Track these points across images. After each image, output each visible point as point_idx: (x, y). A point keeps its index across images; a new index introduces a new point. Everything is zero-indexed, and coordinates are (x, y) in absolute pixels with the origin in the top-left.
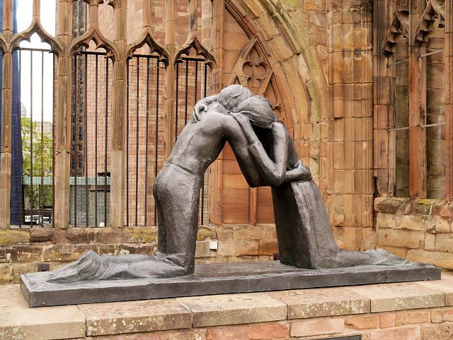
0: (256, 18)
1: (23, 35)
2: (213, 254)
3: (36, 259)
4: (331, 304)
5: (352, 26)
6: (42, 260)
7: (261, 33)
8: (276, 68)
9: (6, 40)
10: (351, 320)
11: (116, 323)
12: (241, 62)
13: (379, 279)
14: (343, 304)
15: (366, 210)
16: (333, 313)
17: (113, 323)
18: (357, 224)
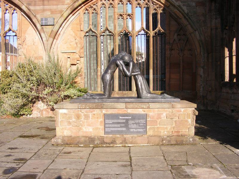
0: (180, 19)
5: (214, 20)
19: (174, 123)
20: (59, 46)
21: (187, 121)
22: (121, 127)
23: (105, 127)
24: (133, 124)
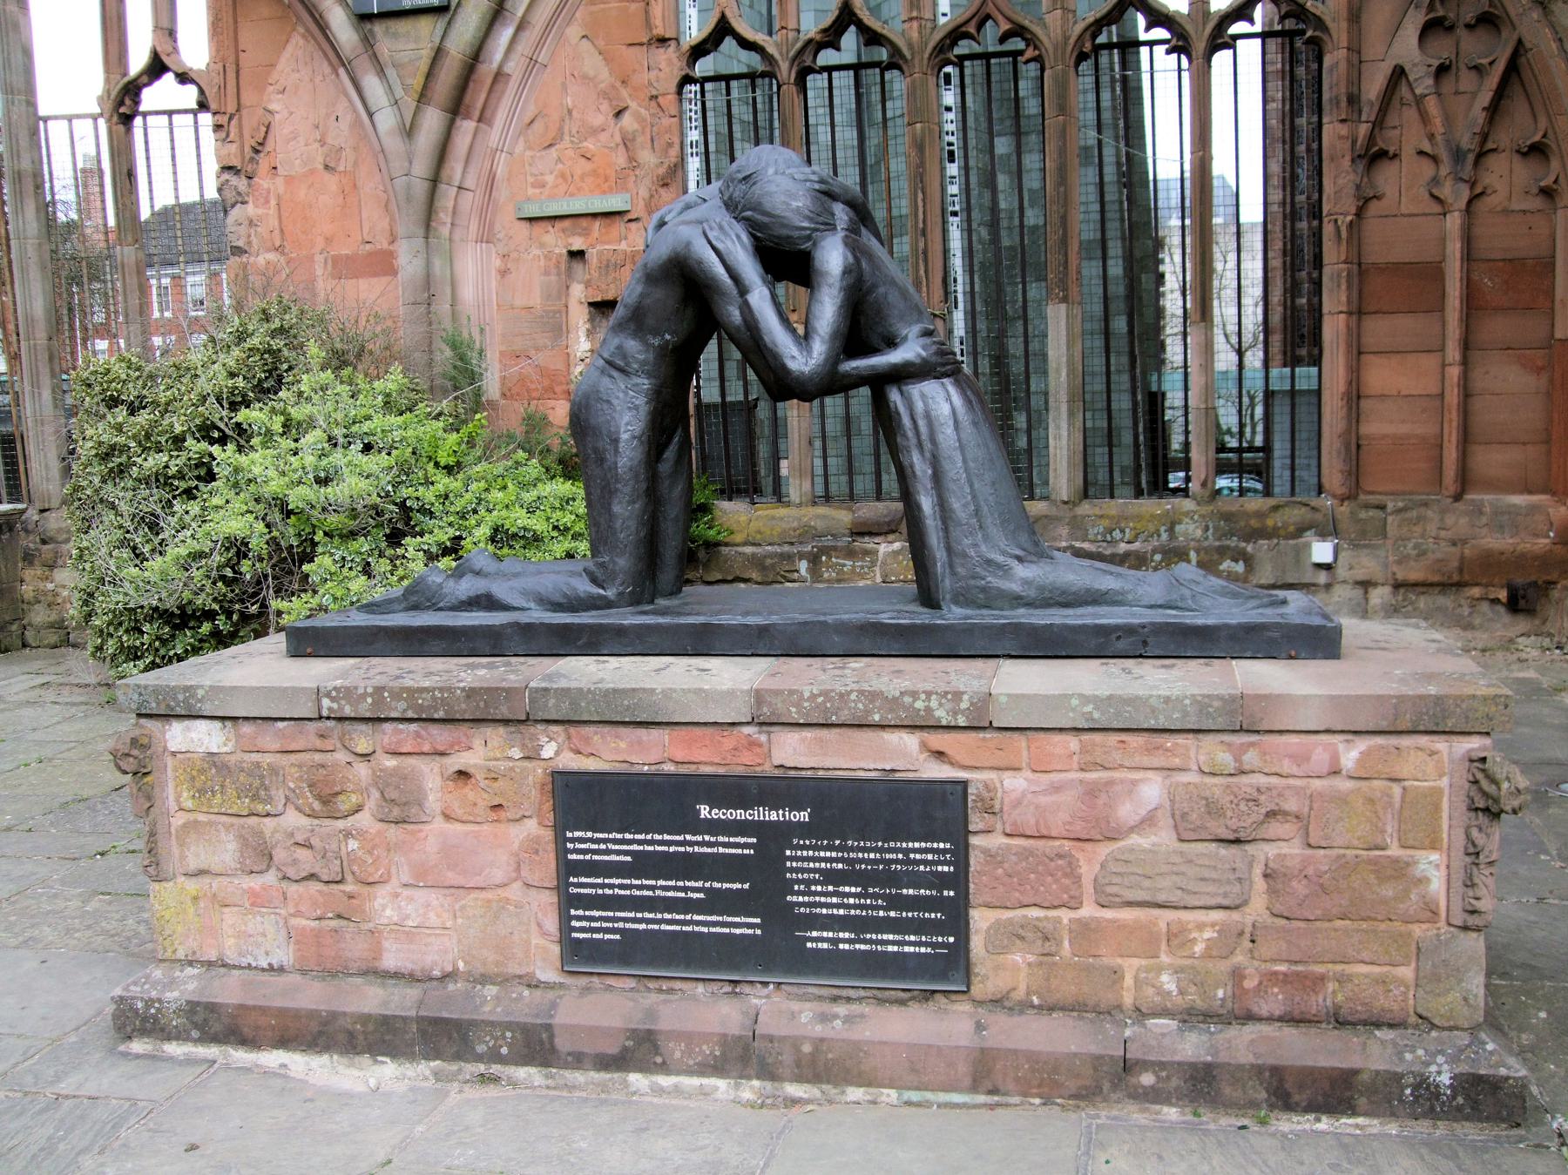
1: (818, 37)
2: (1322, 578)
3: (862, 576)
4: (873, 696)
6: (879, 579)
9: (781, 54)
10: (938, 740)
11: (371, 695)
13: (1121, 645)
14: (908, 699)
16: (877, 717)
17: (365, 695)
19: (1260, 884)
20: (501, 171)
21: (1399, 871)
22: (715, 903)
23: (568, 901)
24: (830, 877)
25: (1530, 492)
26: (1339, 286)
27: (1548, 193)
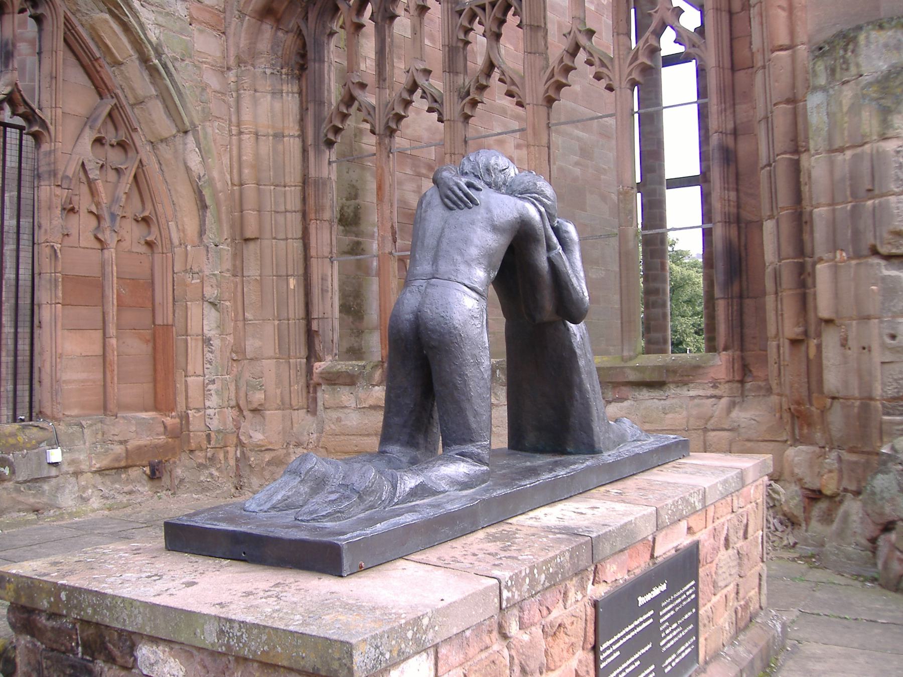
0: (117, 63)
2: (54, 471)
5: (269, 97)
7: (123, 90)
8: (145, 152)
12: (88, 137)
15: (298, 383)
18: (285, 406)
25: (146, 411)
26: (56, 286)
27: (150, 244)
